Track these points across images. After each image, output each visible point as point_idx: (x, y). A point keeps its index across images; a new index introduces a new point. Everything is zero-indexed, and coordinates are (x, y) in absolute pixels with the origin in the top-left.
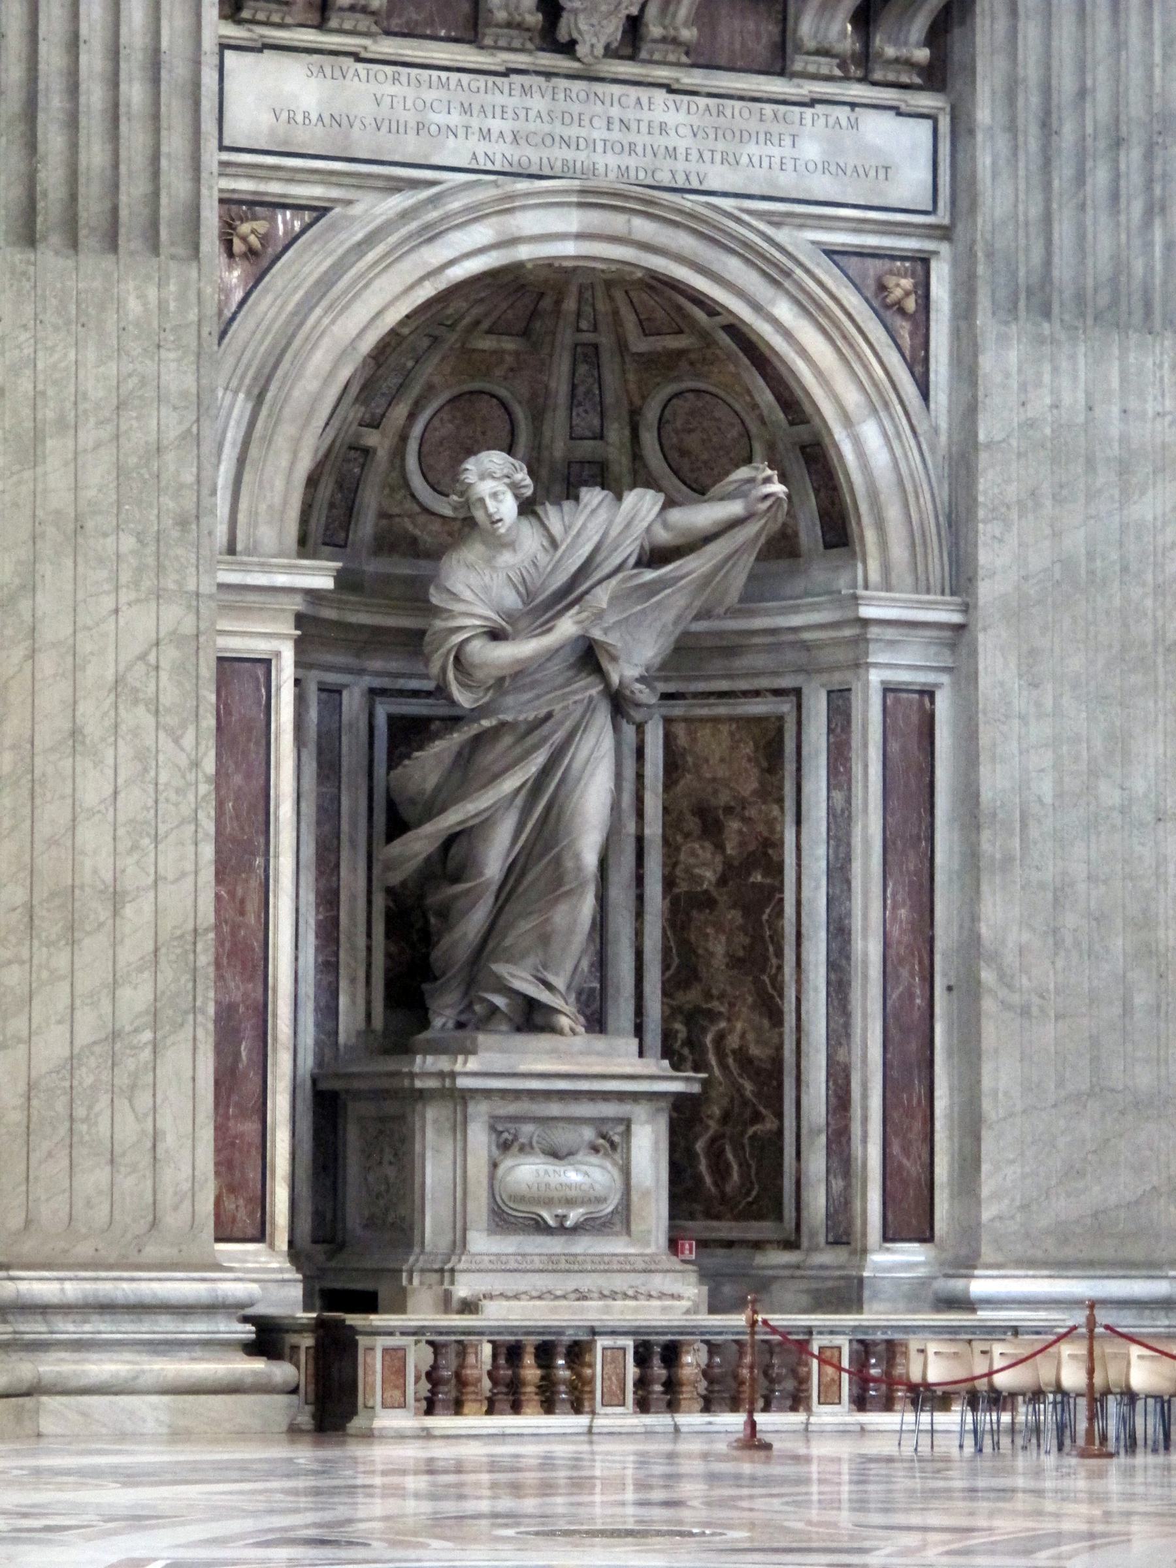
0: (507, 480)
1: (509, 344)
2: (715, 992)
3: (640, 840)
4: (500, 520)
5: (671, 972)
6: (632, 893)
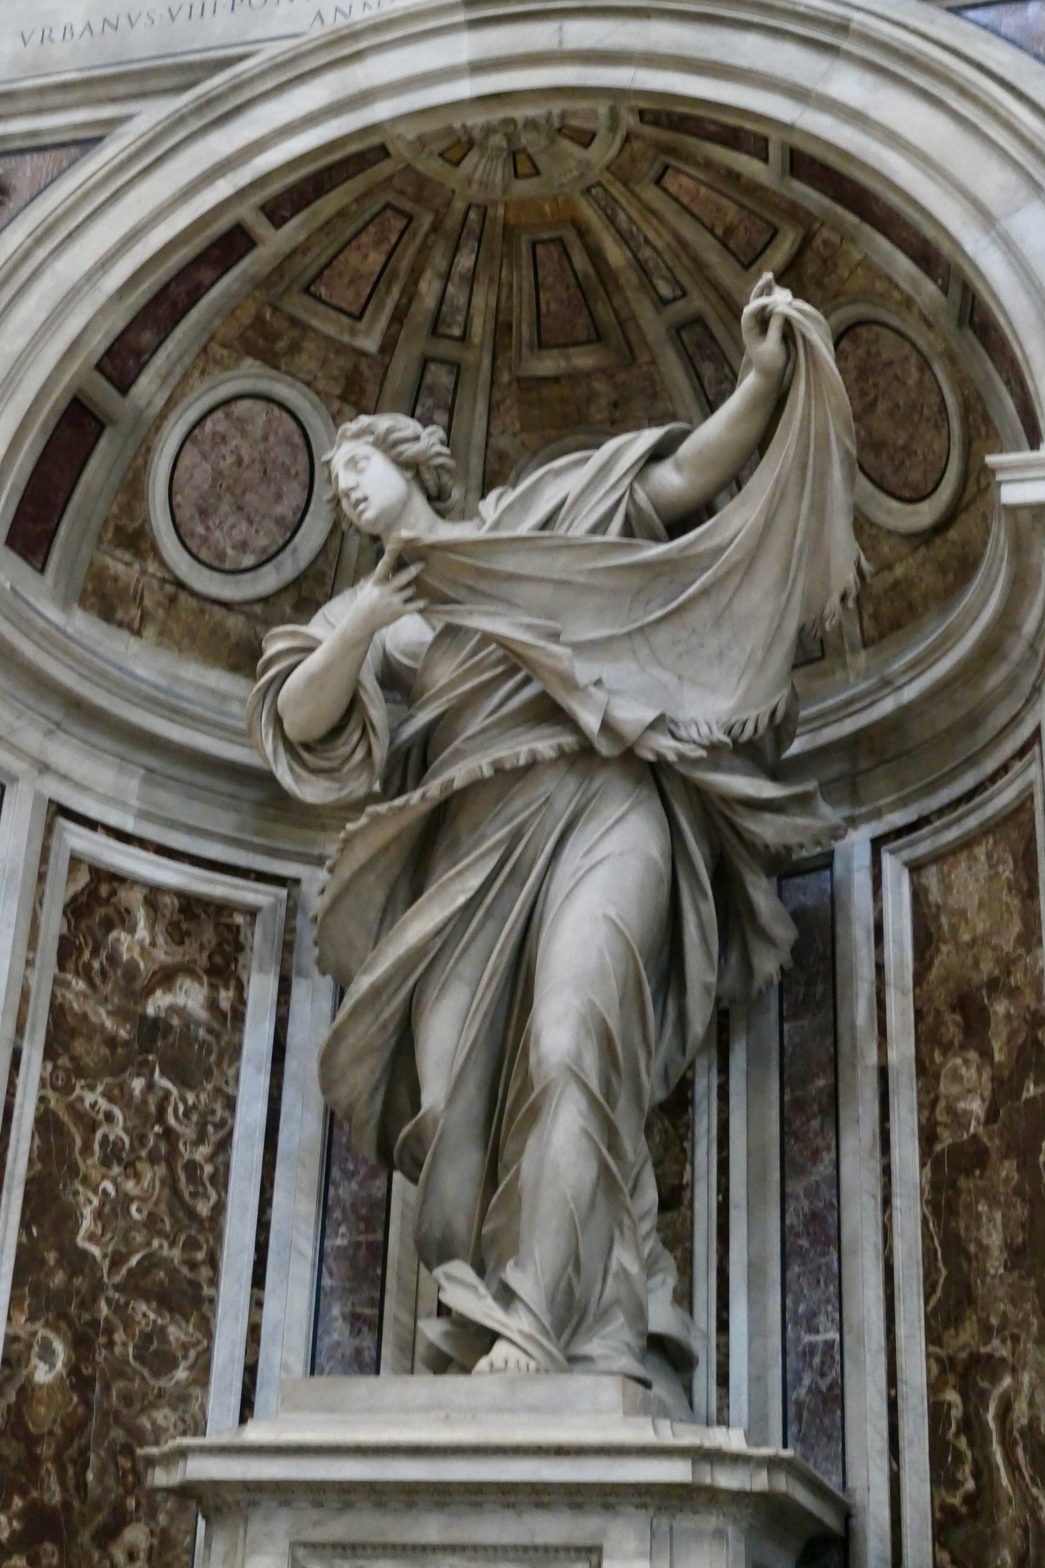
0: (371, 439)
1: (584, 360)
2: (994, 1321)
3: (883, 1072)
4: (365, 499)
5: (939, 1292)
6: (876, 1165)
